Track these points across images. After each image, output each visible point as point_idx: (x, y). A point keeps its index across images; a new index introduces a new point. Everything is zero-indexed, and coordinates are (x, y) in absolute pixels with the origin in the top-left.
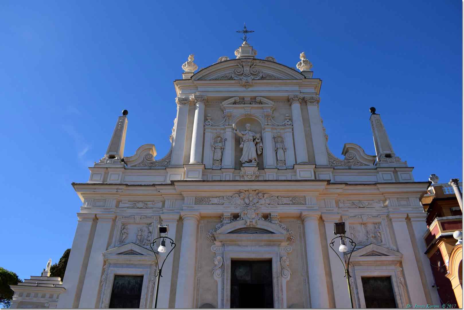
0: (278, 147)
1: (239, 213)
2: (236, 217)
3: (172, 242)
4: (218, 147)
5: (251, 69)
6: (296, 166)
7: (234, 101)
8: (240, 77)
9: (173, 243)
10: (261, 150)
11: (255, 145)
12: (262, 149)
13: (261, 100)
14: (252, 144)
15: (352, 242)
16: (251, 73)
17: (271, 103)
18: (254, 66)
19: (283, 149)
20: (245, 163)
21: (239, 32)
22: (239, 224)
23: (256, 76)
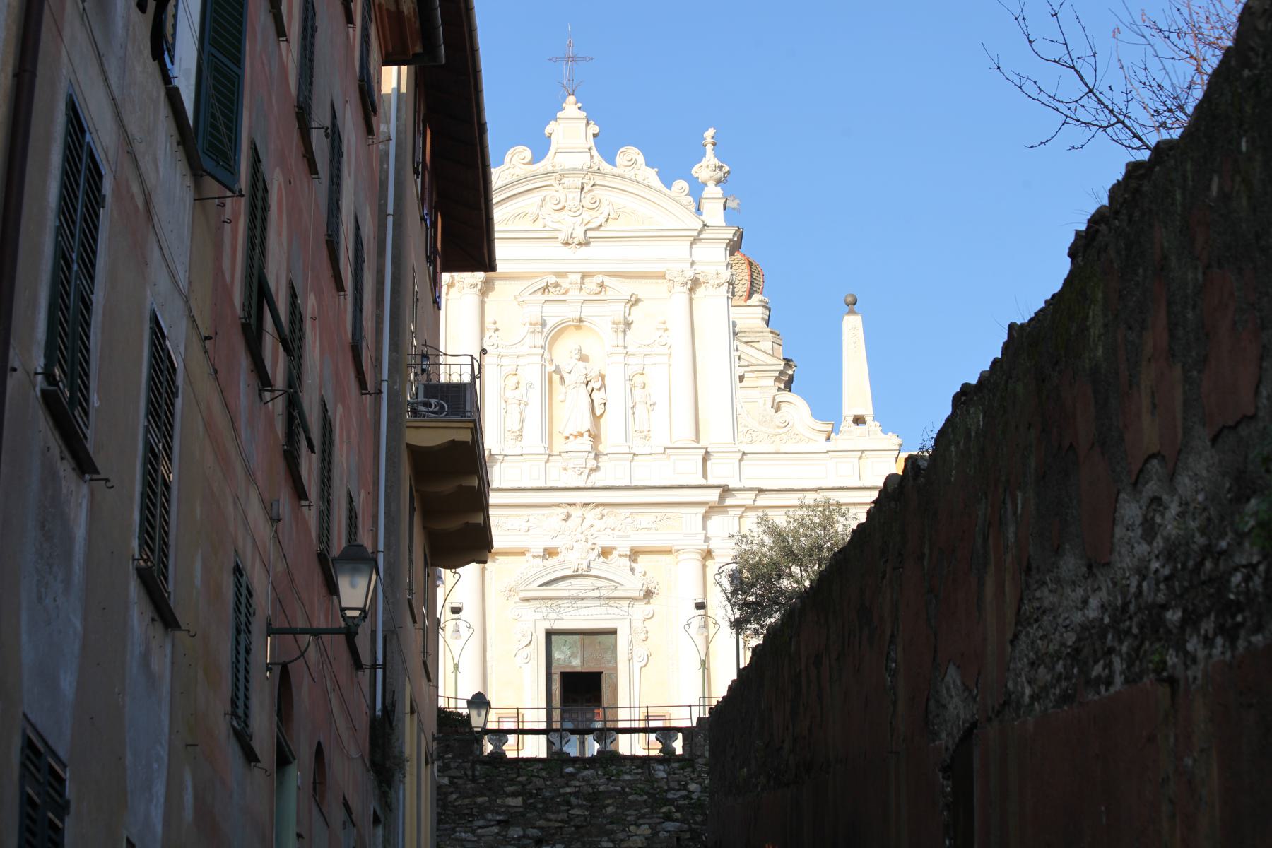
0: (637, 399)
1: (558, 548)
2: (549, 553)
3: (468, 626)
4: (514, 401)
5: (583, 195)
6: (668, 451)
7: (545, 284)
8: (557, 214)
9: (470, 628)
10: (603, 405)
11: (590, 395)
12: (605, 404)
13: (605, 284)
14: (584, 392)
15: (715, 624)
16: (583, 206)
17: (624, 289)
18: (592, 186)
19: (646, 403)
20: (567, 438)
21: (554, 59)
22: (555, 567)
23: (594, 213)
